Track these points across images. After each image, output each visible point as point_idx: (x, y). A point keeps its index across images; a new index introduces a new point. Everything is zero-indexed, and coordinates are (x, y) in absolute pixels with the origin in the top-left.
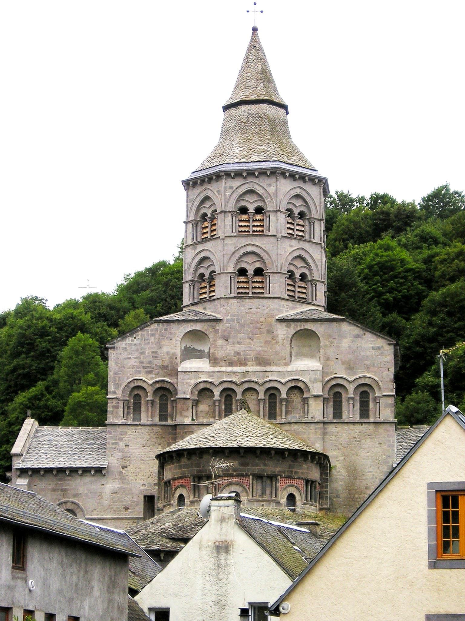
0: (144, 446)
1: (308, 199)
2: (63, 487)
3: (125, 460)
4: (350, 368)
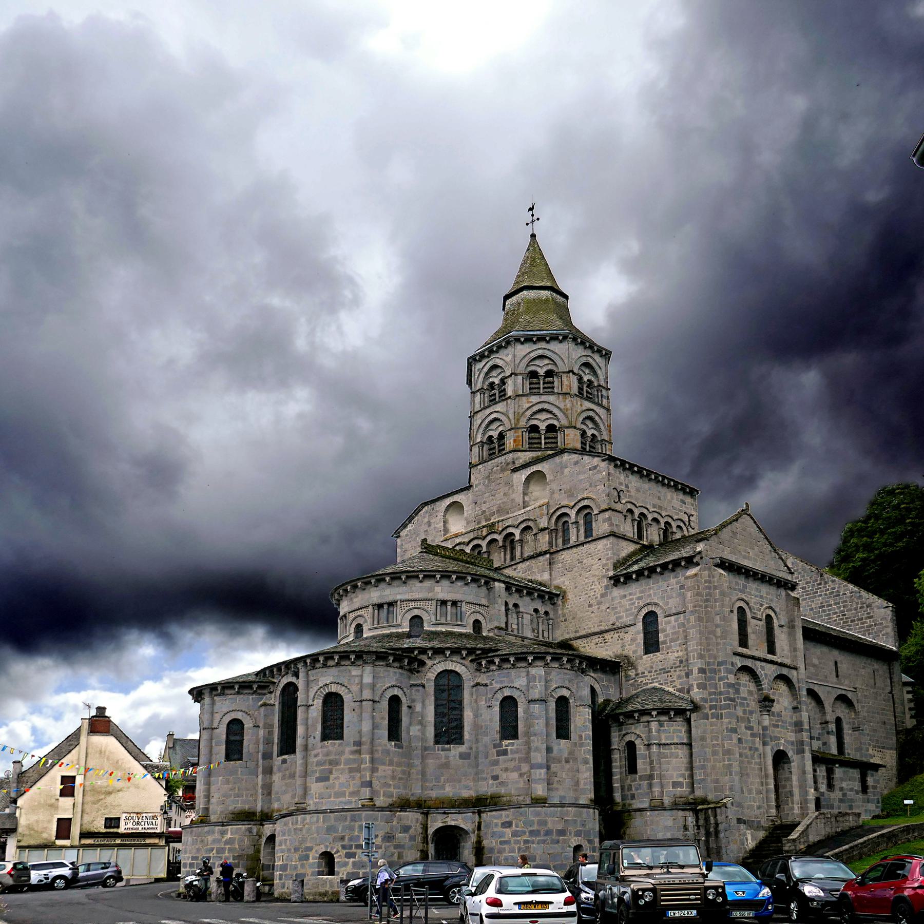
1: (553, 357)
4: (570, 494)
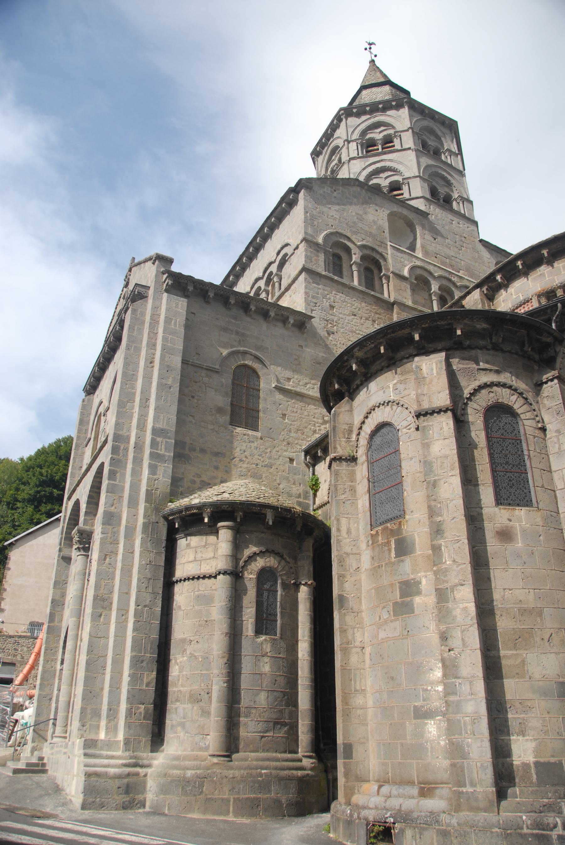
0: (355, 315)
2: (239, 330)
3: (331, 323)
